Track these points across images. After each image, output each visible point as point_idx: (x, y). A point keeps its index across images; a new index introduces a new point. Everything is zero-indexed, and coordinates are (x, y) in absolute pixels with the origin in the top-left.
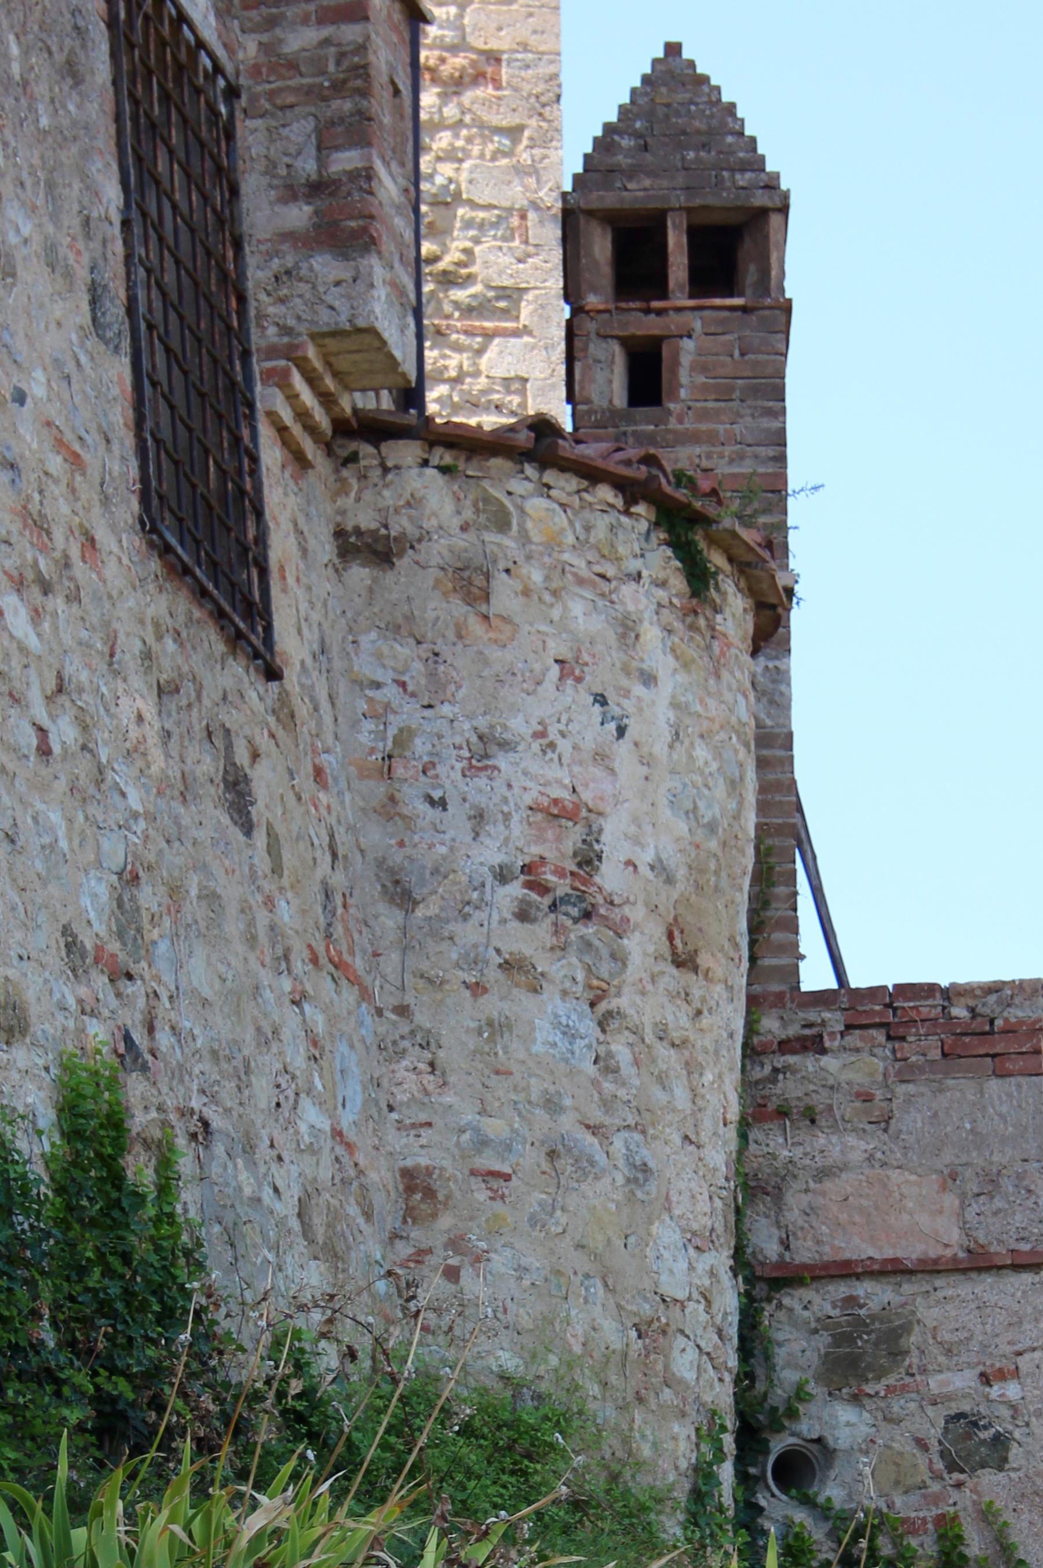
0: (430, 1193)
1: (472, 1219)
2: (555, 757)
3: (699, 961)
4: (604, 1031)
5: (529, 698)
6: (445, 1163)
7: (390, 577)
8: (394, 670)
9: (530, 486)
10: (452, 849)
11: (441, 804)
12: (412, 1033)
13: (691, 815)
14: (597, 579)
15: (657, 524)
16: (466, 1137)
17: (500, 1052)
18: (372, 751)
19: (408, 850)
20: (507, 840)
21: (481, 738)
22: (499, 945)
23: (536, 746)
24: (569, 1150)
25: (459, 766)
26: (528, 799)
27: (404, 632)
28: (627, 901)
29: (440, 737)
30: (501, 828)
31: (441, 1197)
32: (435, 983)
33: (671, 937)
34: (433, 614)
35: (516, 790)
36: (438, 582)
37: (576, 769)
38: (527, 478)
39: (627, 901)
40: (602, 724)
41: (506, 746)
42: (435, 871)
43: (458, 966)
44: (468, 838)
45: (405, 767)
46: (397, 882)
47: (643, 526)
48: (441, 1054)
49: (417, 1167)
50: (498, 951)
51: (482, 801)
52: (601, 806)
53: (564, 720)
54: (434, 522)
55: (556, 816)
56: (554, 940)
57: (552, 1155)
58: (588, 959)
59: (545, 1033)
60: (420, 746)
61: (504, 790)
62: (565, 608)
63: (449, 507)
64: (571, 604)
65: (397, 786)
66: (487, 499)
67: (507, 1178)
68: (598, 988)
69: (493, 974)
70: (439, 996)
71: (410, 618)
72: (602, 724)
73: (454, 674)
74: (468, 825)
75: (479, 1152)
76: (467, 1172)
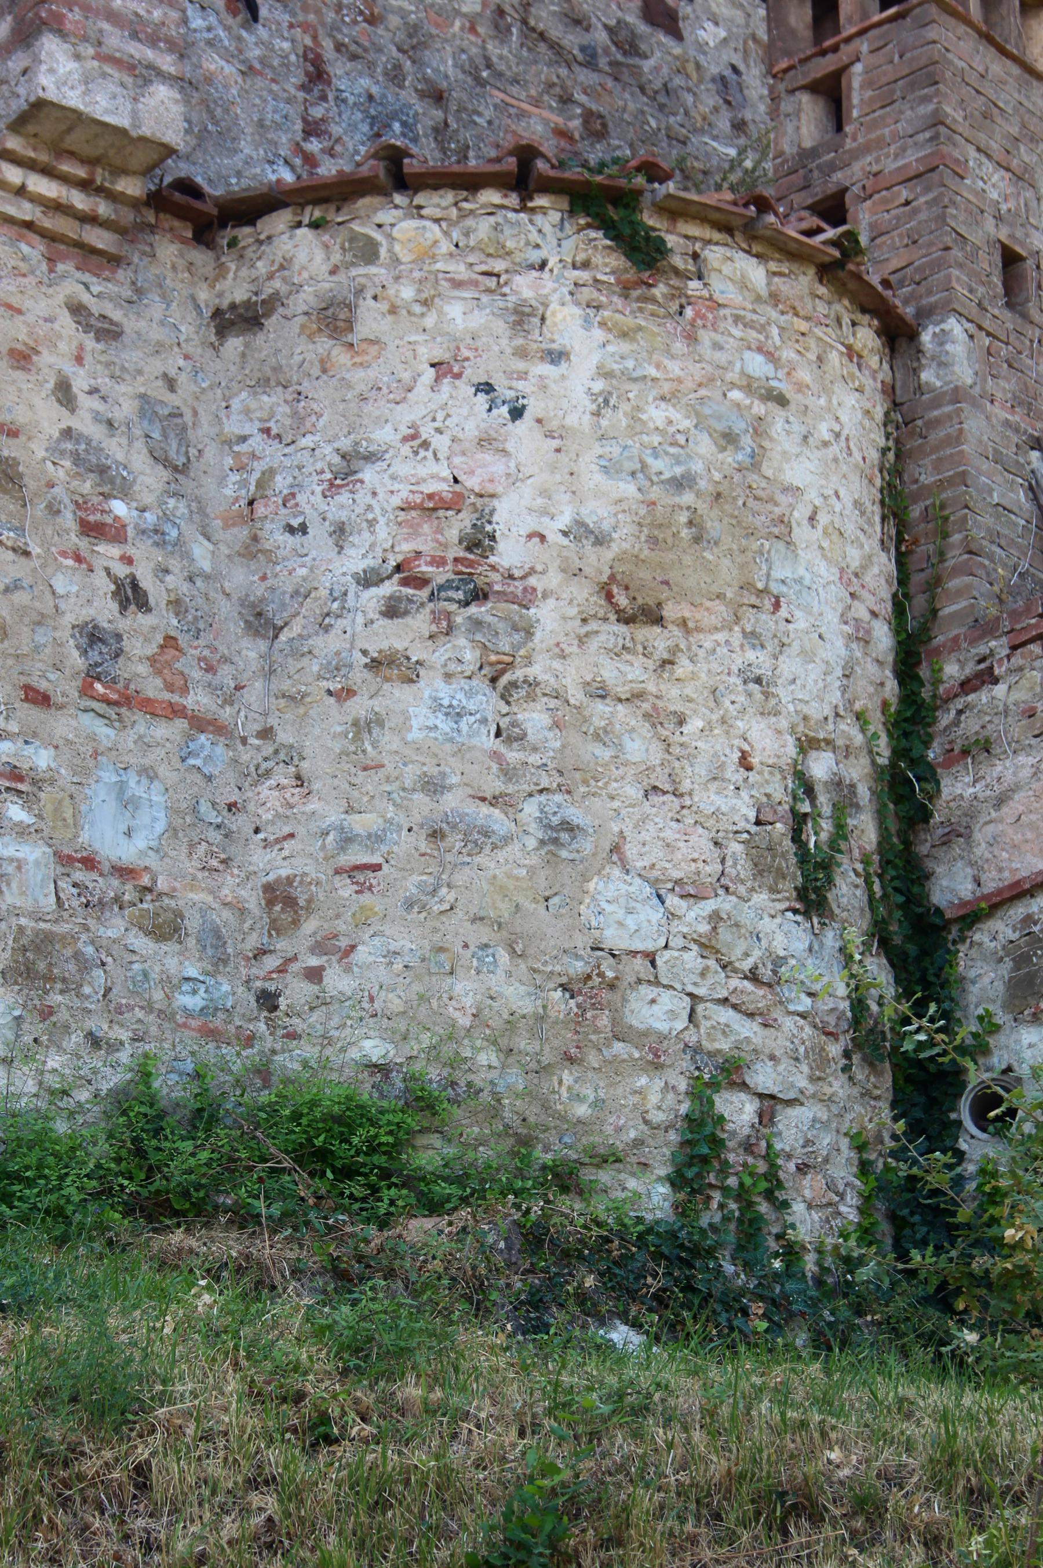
0: (290, 902)
1: (338, 916)
2: (429, 454)
3: (664, 613)
4: (508, 703)
5: (399, 407)
6: (307, 869)
7: (260, 339)
8: (261, 420)
9: (399, 213)
10: (312, 570)
11: (303, 529)
12: (276, 752)
13: (640, 475)
14: (480, 278)
15: (572, 212)
16: (331, 837)
17: (369, 749)
18: (237, 499)
19: (269, 582)
20: (372, 546)
21: (343, 457)
22: (366, 646)
23: (406, 450)
24: (454, 827)
25: (318, 489)
26: (396, 501)
27: (273, 383)
28: (532, 571)
29: (300, 468)
30: (366, 534)
31: (302, 903)
32: (295, 699)
33: (609, 596)
34: (298, 359)
35: (381, 496)
36: (303, 327)
37: (457, 460)
38: (396, 207)
39: (532, 571)
40: (490, 410)
41: (371, 458)
42: (296, 593)
43: (319, 677)
44: (333, 554)
45: (266, 506)
46: (259, 614)
47: (555, 216)
48: (305, 765)
49: (278, 880)
50: (365, 653)
51: (343, 515)
52: (490, 488)
53: (440, 416)
54: (305, 275)
55: (434, 510)
56: (434, 628)
57: (436, 835)
58: (479, 637)
59: (421, 719)
60: (281, 483)
61: (369, 499)
62: (441, 313)
63: (319, 256)
64: (447, 308)
65: (259, 525)
66: (354, 237)
67: (376, 868)
68: (499, 663)
69: (359, 676)
70: (301, 710)
71: (277, 369)
72: (490, 410)
73: (315, 406)
74: (330, 542)
75: (343, 849)
76: (331, 872)
